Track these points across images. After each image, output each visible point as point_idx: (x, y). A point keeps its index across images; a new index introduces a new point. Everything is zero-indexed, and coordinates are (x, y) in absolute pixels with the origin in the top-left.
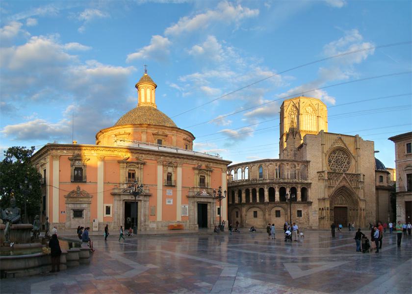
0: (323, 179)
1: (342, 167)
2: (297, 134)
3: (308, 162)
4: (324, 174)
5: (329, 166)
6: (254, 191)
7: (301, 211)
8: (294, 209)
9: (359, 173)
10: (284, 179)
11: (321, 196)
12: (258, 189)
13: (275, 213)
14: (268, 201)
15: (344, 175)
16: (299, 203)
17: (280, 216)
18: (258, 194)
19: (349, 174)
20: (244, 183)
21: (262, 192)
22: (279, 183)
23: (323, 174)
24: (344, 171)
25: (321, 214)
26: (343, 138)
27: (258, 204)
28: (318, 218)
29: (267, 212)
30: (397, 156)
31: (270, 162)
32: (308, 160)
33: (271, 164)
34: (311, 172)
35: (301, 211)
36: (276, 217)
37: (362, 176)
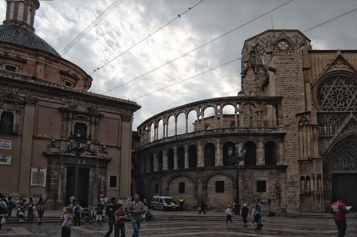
1: (346, 105)
2: (260, 68)
5: (320, 104)
6: (181, 151)
7: (264, 182)
11: (305, 156)
13: (215, 186)
16: (261, 168)
18: (186, 155)
20: (166, 141)
26: (345, 56)
27: (186, 170)
29: (201, 184)
34: (285, 115)
35: (264, 182)
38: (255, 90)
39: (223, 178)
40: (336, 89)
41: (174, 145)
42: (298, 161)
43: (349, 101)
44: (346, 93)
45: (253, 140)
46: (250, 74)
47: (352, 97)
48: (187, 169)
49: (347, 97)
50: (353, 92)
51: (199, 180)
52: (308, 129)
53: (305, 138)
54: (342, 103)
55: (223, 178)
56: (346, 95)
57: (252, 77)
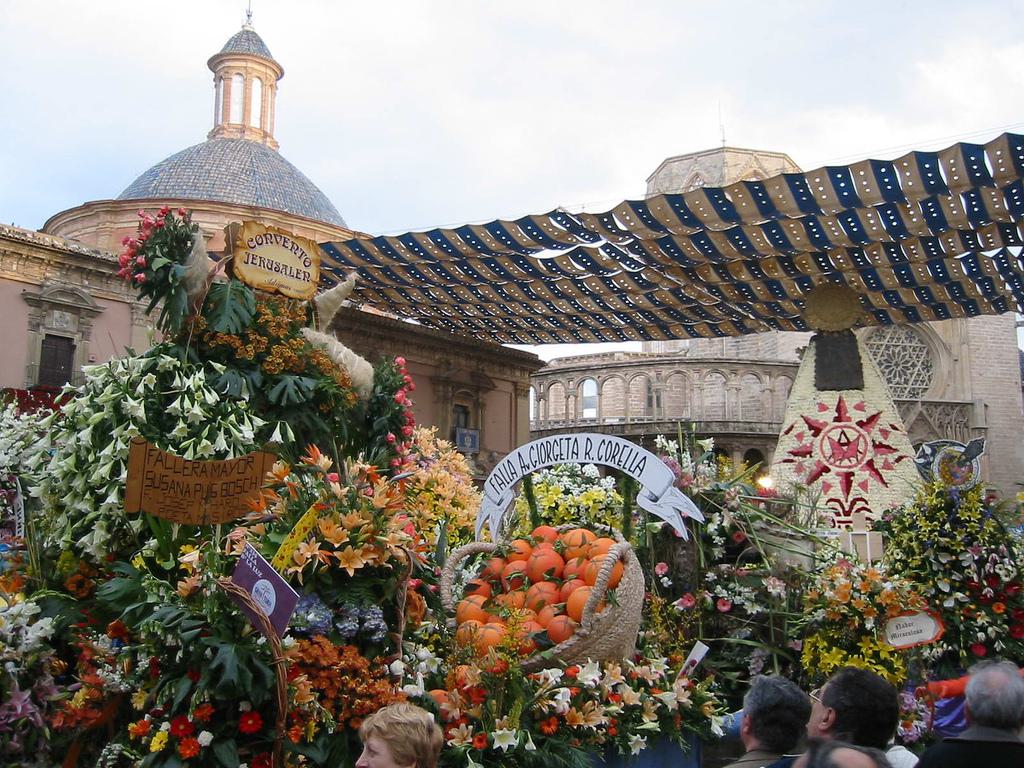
9: (968, 399)
15: (919, 407)
19: (937, 404)
24: (914, 393)
31: (677, 367)
37: (979, 410)
40: (891, 350)
43: (911, 374)
44: (907, 356)
45: (758, 448)
47: (916, 366)
49: (909, 364)
50: (918, 357)
54: (900, 377)
56: (907, 362)
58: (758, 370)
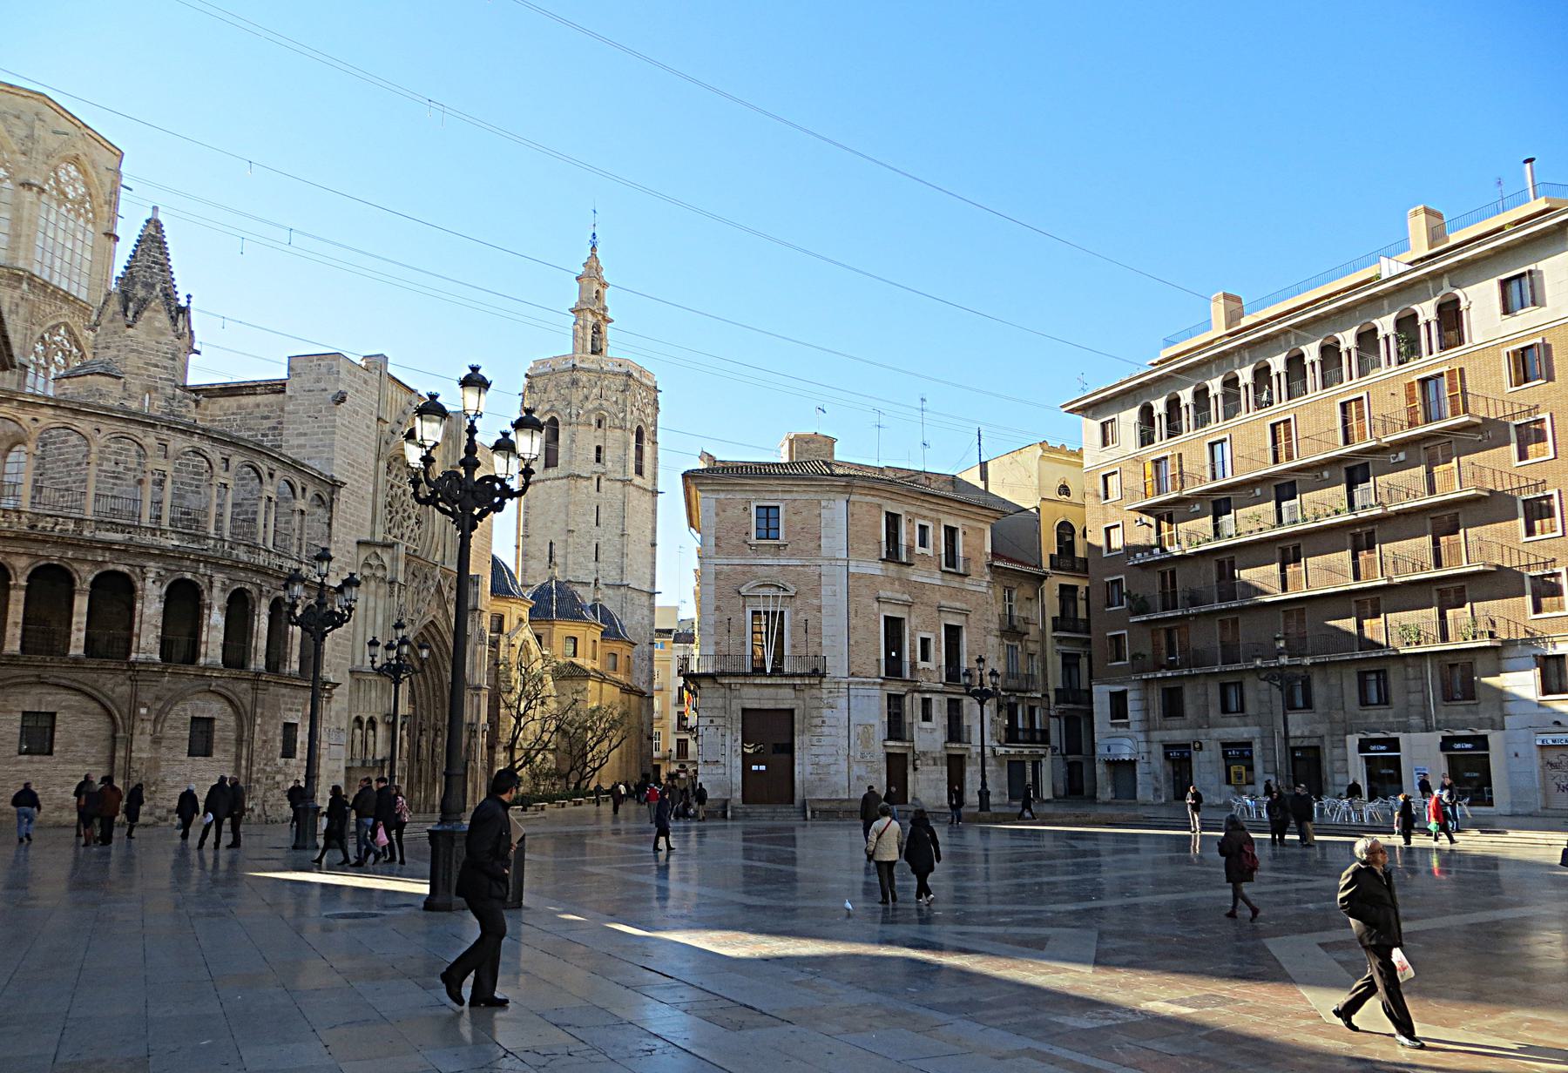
0: (383, 579)
3: (335, 485)
4: (395, 559)
8: (272, 717)
10: (253, 548)
12: (85, 576)
13: (187, 734)
14: (157, 657)
17: (207, 753)
18: (81, 604)
21: (115, 593)
22: (236, 565)
23: (386, 559)
25: (365, 744)
28: (343, 765)
29: (149, 727)
30: (712, 541)
32: (337, 477)
33: (196, 452)
36: (190, 755)
38: (169, 391)
39: (214, 708)
41: (22, 550)
42: (352, 672)
46: (157, 324)
48: (76, 660)
51: (143, 711)
52: (381, 592)
53: (370, 613)
55: (214, 708)
57: (163, 339)
58: (298, 481)
